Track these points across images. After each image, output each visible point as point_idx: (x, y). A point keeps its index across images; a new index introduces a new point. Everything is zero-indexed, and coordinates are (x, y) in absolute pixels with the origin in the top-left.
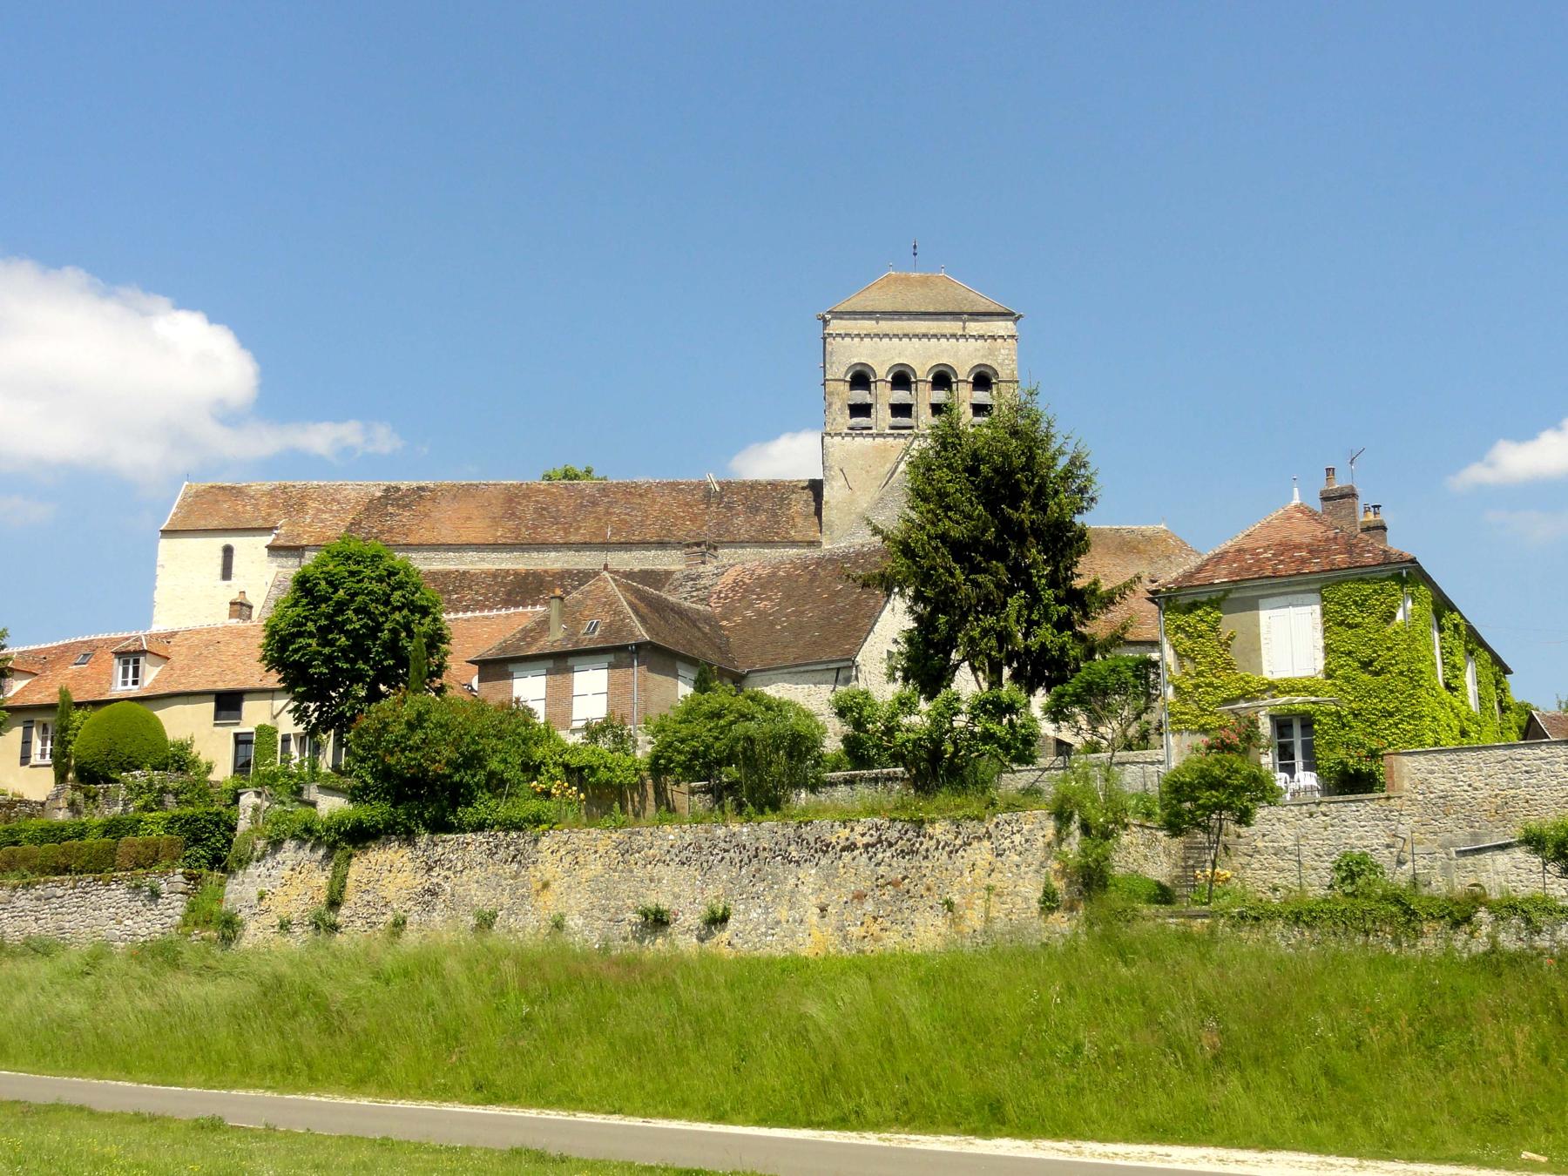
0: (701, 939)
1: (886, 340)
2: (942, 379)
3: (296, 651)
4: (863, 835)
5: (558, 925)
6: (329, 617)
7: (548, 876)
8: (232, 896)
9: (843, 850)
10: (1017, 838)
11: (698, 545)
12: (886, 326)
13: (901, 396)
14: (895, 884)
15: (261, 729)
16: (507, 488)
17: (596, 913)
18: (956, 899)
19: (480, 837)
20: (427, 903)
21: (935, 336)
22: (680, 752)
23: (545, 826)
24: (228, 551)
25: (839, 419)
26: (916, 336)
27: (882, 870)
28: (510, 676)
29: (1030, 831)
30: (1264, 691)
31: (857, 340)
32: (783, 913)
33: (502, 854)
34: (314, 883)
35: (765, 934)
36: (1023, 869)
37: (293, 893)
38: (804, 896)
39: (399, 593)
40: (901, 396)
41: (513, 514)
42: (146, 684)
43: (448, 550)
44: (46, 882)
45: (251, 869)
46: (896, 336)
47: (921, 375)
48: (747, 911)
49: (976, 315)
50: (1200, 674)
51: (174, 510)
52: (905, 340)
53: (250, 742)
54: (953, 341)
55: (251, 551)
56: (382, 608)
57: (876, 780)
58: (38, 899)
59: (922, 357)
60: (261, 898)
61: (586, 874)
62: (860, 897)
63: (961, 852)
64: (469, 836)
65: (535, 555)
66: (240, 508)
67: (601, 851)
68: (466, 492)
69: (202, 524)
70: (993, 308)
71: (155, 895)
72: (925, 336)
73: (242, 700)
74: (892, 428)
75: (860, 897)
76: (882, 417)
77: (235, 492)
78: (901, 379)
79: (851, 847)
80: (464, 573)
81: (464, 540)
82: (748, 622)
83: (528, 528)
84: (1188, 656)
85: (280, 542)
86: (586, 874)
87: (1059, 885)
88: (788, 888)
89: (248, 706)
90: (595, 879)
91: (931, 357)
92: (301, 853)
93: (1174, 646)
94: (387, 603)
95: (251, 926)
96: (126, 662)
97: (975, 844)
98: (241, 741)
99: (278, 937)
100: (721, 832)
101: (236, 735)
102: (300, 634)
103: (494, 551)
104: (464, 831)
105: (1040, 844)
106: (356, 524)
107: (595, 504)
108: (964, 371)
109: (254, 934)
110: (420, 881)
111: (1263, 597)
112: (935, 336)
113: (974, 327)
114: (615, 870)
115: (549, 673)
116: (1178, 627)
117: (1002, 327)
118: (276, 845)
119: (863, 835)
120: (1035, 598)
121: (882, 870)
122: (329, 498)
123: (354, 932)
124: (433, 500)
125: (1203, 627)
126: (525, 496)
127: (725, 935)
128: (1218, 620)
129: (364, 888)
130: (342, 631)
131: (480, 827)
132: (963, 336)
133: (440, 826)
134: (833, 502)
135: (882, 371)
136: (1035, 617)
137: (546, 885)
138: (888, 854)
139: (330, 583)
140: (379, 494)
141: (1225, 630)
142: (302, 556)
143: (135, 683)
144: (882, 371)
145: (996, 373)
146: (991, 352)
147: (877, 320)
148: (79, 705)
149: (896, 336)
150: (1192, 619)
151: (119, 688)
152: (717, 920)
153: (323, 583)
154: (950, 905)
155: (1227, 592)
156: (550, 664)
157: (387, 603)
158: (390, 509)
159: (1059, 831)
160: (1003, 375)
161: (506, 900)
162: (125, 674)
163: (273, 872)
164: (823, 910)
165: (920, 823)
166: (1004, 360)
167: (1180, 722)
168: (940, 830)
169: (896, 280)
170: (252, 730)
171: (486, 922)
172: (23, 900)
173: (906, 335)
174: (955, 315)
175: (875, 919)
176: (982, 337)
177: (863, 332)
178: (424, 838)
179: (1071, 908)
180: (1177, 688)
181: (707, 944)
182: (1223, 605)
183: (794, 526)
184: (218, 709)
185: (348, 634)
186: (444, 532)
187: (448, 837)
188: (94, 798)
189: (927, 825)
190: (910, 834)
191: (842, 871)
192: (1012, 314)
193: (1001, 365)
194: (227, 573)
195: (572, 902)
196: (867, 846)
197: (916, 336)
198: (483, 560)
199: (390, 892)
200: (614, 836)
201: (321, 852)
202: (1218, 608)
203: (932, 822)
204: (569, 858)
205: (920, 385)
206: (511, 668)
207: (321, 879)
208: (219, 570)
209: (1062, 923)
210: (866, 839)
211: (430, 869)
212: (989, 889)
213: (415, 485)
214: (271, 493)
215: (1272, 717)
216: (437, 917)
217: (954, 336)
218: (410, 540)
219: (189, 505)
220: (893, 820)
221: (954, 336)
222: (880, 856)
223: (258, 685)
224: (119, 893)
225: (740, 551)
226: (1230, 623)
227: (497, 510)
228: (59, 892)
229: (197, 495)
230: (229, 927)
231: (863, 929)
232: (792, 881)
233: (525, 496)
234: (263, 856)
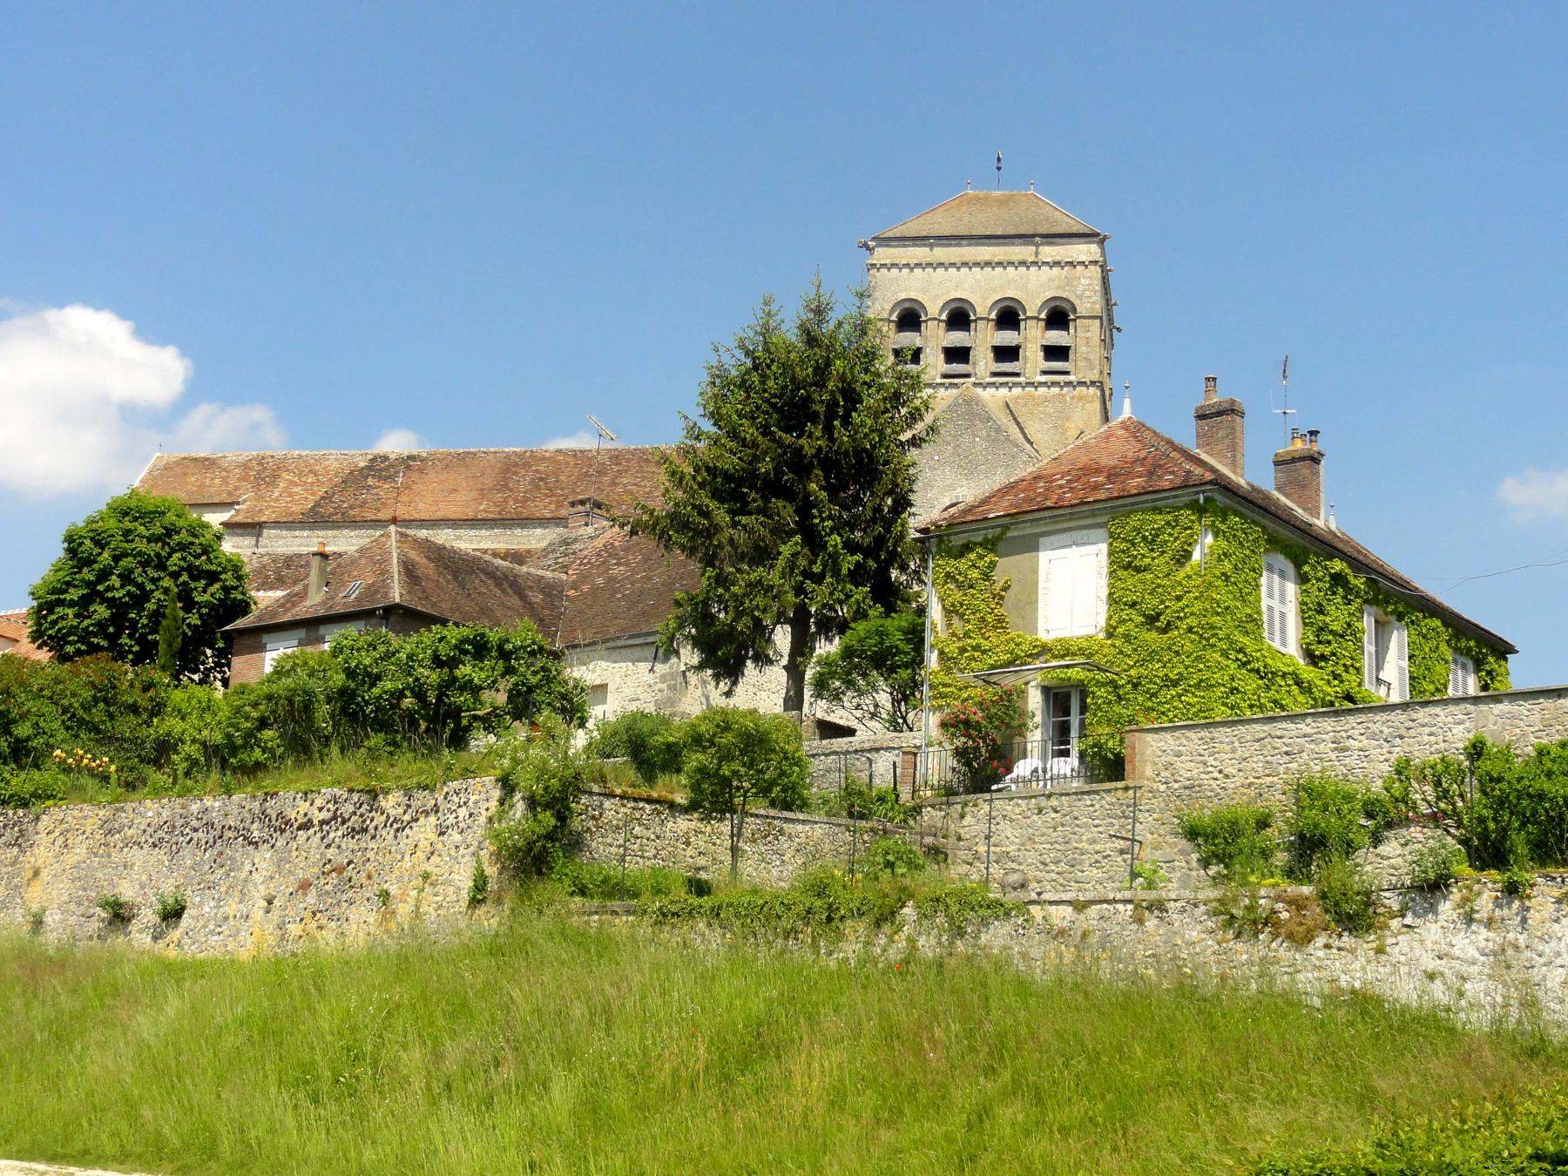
0: (155, 939)
1: (941, 271)
4: (320, 809)
5: (38, 923)
7: (40, 863)
9: (299, 829)
10: (463, 812)
11: (582, 503)
13: (957, 338)
14: (339, 870)
17: (73, 907)
18: (393, 890)
21: (999, 264)
22: (247, 718)
23: (50, 803)
26: (977, 264)
27: (331, 853)
29: (476, 802)
30: (1038, 655)
32: (232, 907)
35: (212, 932)
36: (462, 851)
38: (255, 885)
39: (178, 555)
40: (957, 338)
41: (506, 486)
46: (952, 265)
47: (981, 310)
48: (201, 904)
50: (967, 635)
52: (964, 270)
54: (1022, 269)
56: (152, 573)
59: (982, 289)
61: (71, 859)
62: (305, 886)
63: (407, 831)
65: (518, 532)
66: (208, 481)
70: (1076, 229)
72: (988, 264)
74: (945, 376)
75: (305, 886)
77: (208, 464)
78: (959, 318)
79: (306, 826)
81: (440, 515)
82: (595, 591)
83: (516, 501)
84: (957, 612)
85: (239, 519)
86: (71, 859)
87: (491, 871)
88: (243, 875)
91: (995, 291)
93: (942, 600)
94: (161, 566)
97: (422, 820)
100: (195, 807)
103: (473, 527)
105: (482, 820)
106: (327, 497)
107: (601, 473)
108: (1033, 306)
111: (1044, 534)
112: (999, 264)
113: (1049, 252)
116: (948, 575)
117: (1085, 251)
119: (320, 809)
120: (814, 541)
121: (331, 853)
122: (306, 468)
124: (421, 470)
125: (975, 574)
126: (527, 465)
127: (176, 934)
128: (992, 565)
130: (104, 600)
132: (1034, 263)
135: (934, 307)
136: (817, 569)
137: (36, 873)
138: (340, 833)
139: (97, 543)
140: (362, 464)
141: (999, 577)
142: (259, 535)
144: (934, 307)
145: (1074, 310)
146: (1069, 281)
147: (931, 246)
149: (952, 265)
150: (963, 564)
152: (173, 914)
153: (88, 542)
154: (385, 896)
155: (1006, 528)
156: (302, 633)
157: (161, 566)
159: (502, 802)
164: (270, 902)
165: (373, 794)
166: (1084, 293)
167: (943, 696)
168: (391, 803)
173: (965, 264)
175: (314, 914)
176: (1057, 264)
177: (913, 262)
179: (499, 901)
180: (942, 653)
181: (161, 944)
182: (1001, 546)
185: (111, 603)
186: (421, 506)
189: (381, 797)
190: (365, 806)
191: (295, 854)
192: (1097, 235)
193: (1080, 297)
196: (322, 823)
197: (977, 264)
198: (459, 538)
200: (101, 813)
202: (992, 550)
203: (386, 792)
204: (60, 841)
206: (265, 638)
209: (490, 919)
210: (324, 815)
212: (426, 876)
215: (1046, 690)
217: (1023, 263)
219: (156, 478)
220: (351, 791)
221: (1023, 263)
222: (332, 835)
226: (1007, 567)
227: (489, 481)
229: (167, 467)
231: (301, 927)
232: (248, 867)
233: (527, 465)
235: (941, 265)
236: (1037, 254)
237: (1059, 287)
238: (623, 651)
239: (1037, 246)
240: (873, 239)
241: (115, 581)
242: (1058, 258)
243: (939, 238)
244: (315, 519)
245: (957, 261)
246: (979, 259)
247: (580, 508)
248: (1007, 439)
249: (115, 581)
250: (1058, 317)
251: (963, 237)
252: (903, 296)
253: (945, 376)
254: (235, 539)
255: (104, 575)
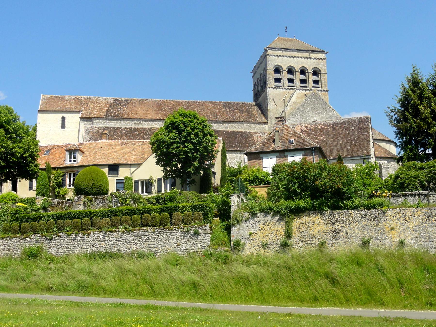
1: (285, 58)
2: (303, 72)
3: (173, 149)
5: (402, 243)
6: (186, 137)
7: (393, 225)
8: (235, 234)
12: (285, 53)
15: (126, 178)
16: (156, 101)
19: (356, 211)
20: (335, 236)
21: (301, 57)
24: (63, 119)
25: (272, 83)
28: (261, 158)
31: (276, 57)
33: (368, 217)
34: (276, 229)
37: (266, 233)
41: (162, 110)
42: (79, 161)
43: (144, 121)
44: (140, 230)
45: (243, 224)
46: (289, 57)
47: (297, 70)
49: (313, 51)
51: (40, 104)
52: (292, 58)
53: (123, 183)
55: (73, 119)
57: (415, 195)
58: (136, 236)
60: (250, 235)
64: (351, 211)
67: (417, 216)
68: (142, 102)
69: (52, 109)
70: (317, 50)
71: (196, 234)
72: (298, 57)
73: (118, 168)
74: (288, 86)
76: (285, 83)
78: (290, 71)
80: (150, 129)
81: (148, 117)
85: (84, 116)
89: (121, 170)
90: (417, 226)
92: (267, 218)
95: (248, 246)
96: (70, 154)
98: (119, 182)
99: (262, 250)
101: (116, 180)
102: (174, 142)
104: (348, 209)
109: (249, 249)
110: (329, 228)
112: (301, 57)
113: (313, 55)
114: (426, 223)
115: (277, 157)
118: (254, 215)
123: (299, 247)
129: (301, 231)
131: (356, 208)
133: (335, 207)
134: (271, 110)
140: (112, 101)
142: (92, 121)
143: (74, 161)
145: (320, 71)
146: (318, 64)
147: (283, 51)
148: (55, 169)
149: (289, 57)
151: (68, 164)
156: (278, 154)
158: (119, 107)
160: (322, 71)
161: (373, 234)
162: (70, 158)
163: (254, 225)
166: (322, 66)
169: (282, 39)
170: (123, 178)
171: (365, 244)
172: (127, 237)
173: (292, 57)
174: (307, 51)
176: (315, 58)
177: (278, 55)
178: (328, 212)
183: (257, 117)
184: (110, 170)
185: (192, 143)
187: (340, 211)
188: (91, 201)
193: (321, 68)
194: (63, 126)
195: (407, 235)
198: (156, 124)
199: (315, 232)
200: (423, 211)
201: (277, 218)
204: (402, 219)
205: (297, 73)
206: (261, 155)
207: (281, 228)
208: (60, 125)
211: (333, 223)
213: (124, 99)
214: (74, 99)
216: (340, 241)
217: (307, 58)
218: (130, 117)
219: (45, 102)
221: (307, 58)
223: (124, 162)
224: (178, 234)
225: (242, 125)
228: (146, 234)
229: (47, 99)
230: (237, 246)
234: (248, 219)
235: (286, 56)
236: (310, 55)
237: (316, 65)
238: (351, 161)
239: (310, 53)
240: (268, 48)
241: (192, 136)
242: (315, 57)
243: (285, 49)
244: (108, 117)
245: (294, 56)
246: (295, 56)
247: (279, 119)
248: (326, 105)
249: (192, 136)
250: (315, 73)
251: (278, 49)
252: (276, 64)
253: (301, 87)
254: (84, 122)
255: (189, 134)
